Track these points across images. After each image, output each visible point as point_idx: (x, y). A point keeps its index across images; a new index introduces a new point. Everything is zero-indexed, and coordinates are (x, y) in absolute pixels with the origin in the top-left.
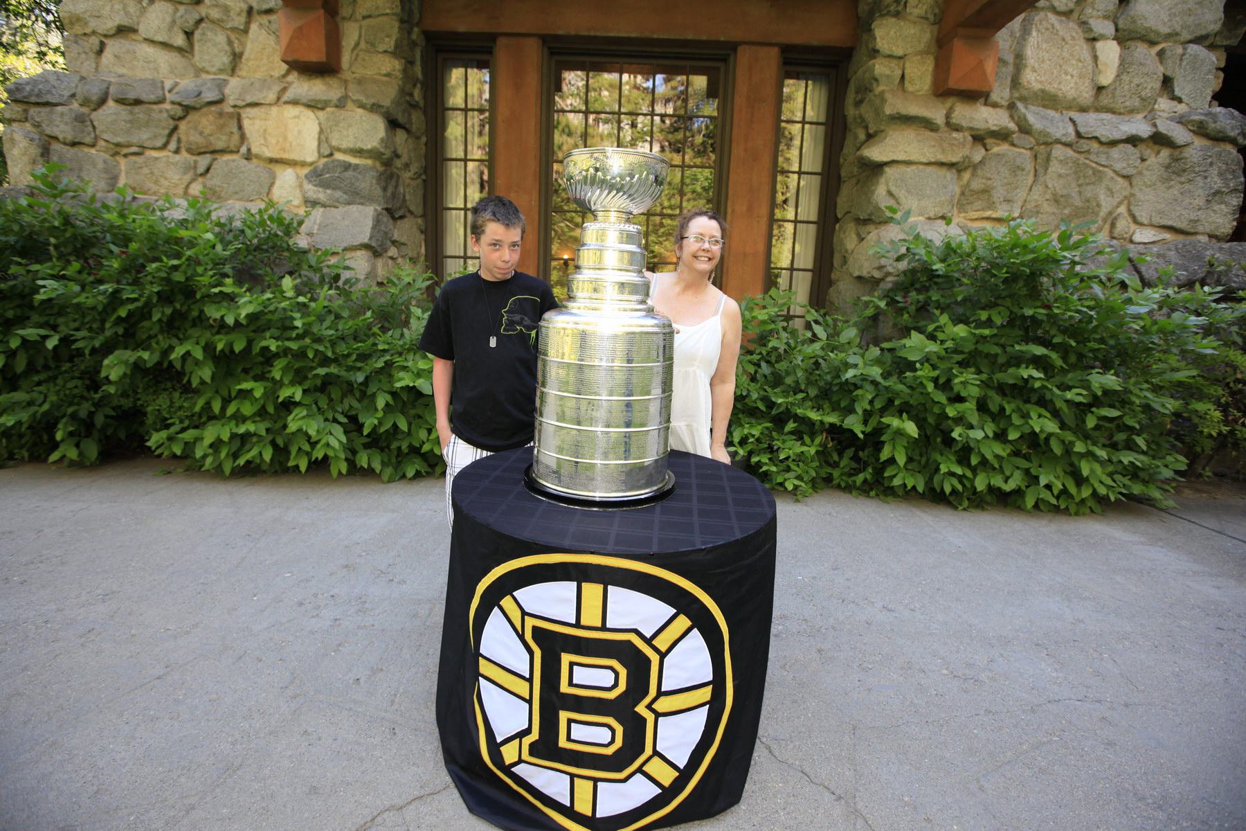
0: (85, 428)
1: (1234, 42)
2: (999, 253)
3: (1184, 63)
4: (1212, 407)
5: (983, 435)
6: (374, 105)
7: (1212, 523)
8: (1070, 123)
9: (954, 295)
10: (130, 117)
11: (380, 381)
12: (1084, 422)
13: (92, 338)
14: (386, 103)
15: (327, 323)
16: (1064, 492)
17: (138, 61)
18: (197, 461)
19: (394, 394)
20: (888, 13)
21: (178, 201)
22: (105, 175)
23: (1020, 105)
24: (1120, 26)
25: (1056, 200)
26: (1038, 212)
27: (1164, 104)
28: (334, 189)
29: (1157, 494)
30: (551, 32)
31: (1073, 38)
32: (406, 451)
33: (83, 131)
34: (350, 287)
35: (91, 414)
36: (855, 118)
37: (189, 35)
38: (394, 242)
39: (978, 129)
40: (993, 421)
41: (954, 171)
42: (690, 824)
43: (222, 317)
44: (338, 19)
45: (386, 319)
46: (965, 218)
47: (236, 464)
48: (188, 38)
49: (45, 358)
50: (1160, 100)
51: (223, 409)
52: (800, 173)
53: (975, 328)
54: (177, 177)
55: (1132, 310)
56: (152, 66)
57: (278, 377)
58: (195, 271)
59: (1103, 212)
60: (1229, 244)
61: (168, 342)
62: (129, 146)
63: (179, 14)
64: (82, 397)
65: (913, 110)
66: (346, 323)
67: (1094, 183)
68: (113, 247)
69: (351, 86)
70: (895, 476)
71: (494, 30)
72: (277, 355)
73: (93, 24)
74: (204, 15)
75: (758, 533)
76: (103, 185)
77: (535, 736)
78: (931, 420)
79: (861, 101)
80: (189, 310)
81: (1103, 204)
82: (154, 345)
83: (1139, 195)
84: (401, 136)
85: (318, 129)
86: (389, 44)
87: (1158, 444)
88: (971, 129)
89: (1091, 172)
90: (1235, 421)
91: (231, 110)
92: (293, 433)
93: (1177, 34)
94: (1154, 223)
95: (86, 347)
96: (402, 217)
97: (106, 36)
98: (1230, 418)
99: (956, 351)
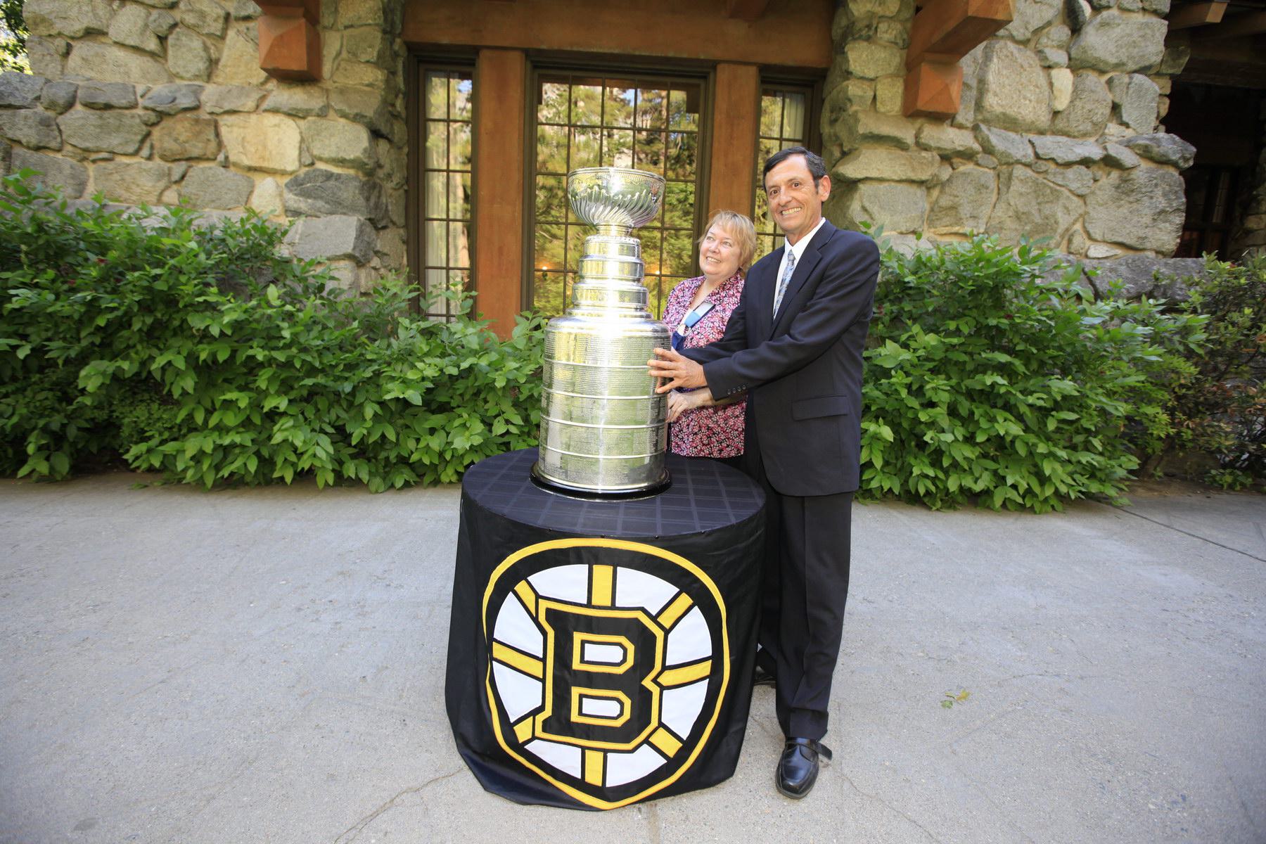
0: (57, 440)
1: (1178, 71)
2: (965, 266)
3: (1130, 92)
4: (1159, 410)
5: (953, 438)
7: (1161, 518)
8: (1029, 145)
9: (925, 306)
10: (99, 122)
11: (367, 391)
12: (1046, 425)
13: (69, 349)
14: (370, 113)
15: (314, 334)
16: (1029, 491)
17: (108, 64)
18: (177, 474)
19: (382, 404)
20: (860, 38)
21: (155, 209)
22: (72, 181)
23: (983, 127)
24: (1073, 55)
25: (1018, 217)
26: (1001, 228)
27: (1113, 129)
28: (315, 198)
29: (1112, 492)
30: (536, 46)
31: (1031, 66)
32: (395, 461)
33: (48, 136)
34: (335, 298)
35: (64, 426)
36: (830, 136)
37: (162, 39)
38: (376, 253)
39: (946, 149)
40: (963, 426)
41: (924, 188)
42: (692, 793)
43: (207, 327)
44: (319, 28)
45: (372, 330)
46: (934, 233)
47: (219, 476)
48: (161, 43)
49: (13, 369)
50: (1110, 125)
51: (206, 422)
53: (945, 337)
54: (150, 184)
55: (1088, 320)
56: (122, 70)
57: (263, 386)
58: (177, 279)
59: (1060, 231)
60: (1174, 260)
61: (148, 352)
62: (98, 151)
63: (152, 18)
64: (53, 409)
65: (886, 130)
66: (331, 334)
67: (1052, 202)
68: (89, 255)
69: (333, 96)
70: (872, 479)
71: (478, 43)
72: (261, 365)
73: (59, 26)
74: (178, 19)
75: (751, 519)
76: (70, 191)
78: (905, 425)
79: (836, 120)
80: (170, 319)
81: (1060, 220)
82: (133, 355)
83: (1093, 214)
84: (383, 146)
85: (298, 138)
86: (372, 54)
87: (1113, 446)
88: (939, 148)
89: (1049, 191)
90: (1181, 424)
91: (208, 117)
92: (278, 444)
93: (1123, 64)
94: (1107, 239)
95: (58, 358)
96: (384, 228)
97: (73, 38)
98: (1176, 421)
99: (927, 359)
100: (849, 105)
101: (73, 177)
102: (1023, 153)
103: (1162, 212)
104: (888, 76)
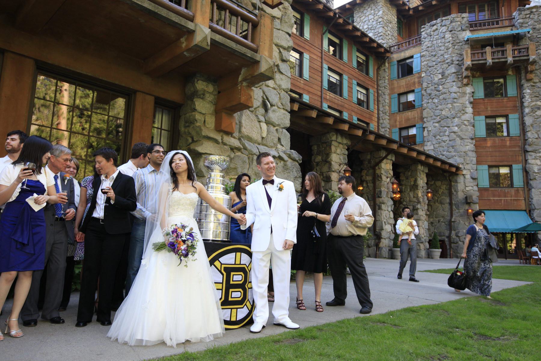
20: (200, 97)
27: (279, 146)
31: (255, 120)
36: (185, 132)
77: (223, 299)
88: (230, 145)
93: (280, 125)
100: (196, 122)
103: (296, 177)
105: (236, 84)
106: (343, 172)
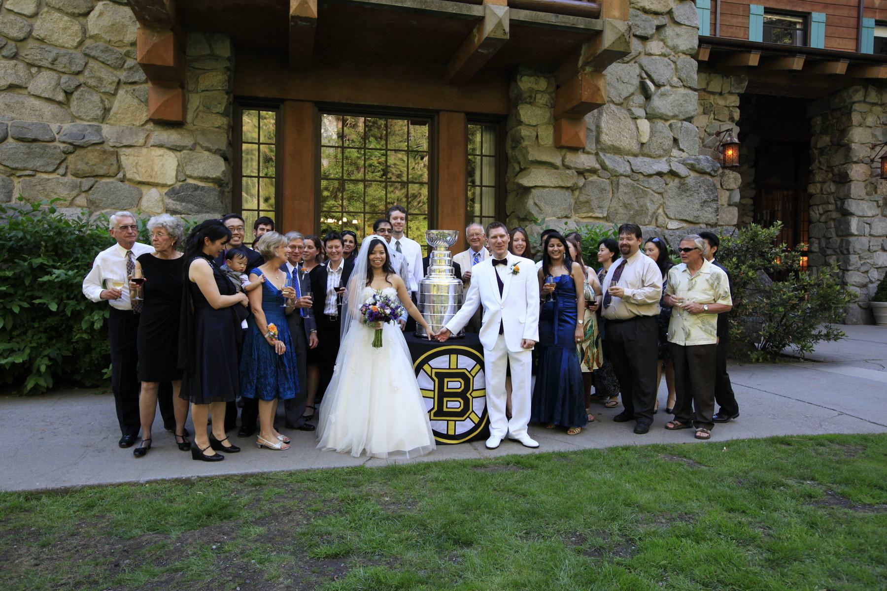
1: (742, 91)
6: (217, 149)
20: (526, 103)
23: (601, 154)
25: (625, 206)
27: (675, 152)
28: (187, 202)
31: (625, 118)
37: (68, 94)
41: (570, 191)
52: (481, 186)
56: (37, 113)
59: (650, 213)
62: (24, 170)
65: (544, 158)
67: (643, 197)
79: (516, 147)
81: (649, 208)
83: (668, 203)
86: (221, 108)
88: (576, 168)
91: (112, 149)
101: (4, 187)
102: (623, 170)
103: (705, 202)
104: (543, 124)
105: (576, 72)
106: (880, 160)
